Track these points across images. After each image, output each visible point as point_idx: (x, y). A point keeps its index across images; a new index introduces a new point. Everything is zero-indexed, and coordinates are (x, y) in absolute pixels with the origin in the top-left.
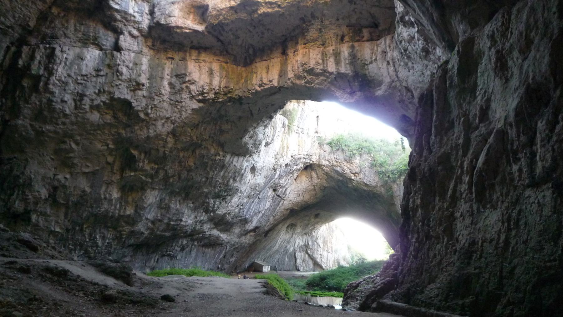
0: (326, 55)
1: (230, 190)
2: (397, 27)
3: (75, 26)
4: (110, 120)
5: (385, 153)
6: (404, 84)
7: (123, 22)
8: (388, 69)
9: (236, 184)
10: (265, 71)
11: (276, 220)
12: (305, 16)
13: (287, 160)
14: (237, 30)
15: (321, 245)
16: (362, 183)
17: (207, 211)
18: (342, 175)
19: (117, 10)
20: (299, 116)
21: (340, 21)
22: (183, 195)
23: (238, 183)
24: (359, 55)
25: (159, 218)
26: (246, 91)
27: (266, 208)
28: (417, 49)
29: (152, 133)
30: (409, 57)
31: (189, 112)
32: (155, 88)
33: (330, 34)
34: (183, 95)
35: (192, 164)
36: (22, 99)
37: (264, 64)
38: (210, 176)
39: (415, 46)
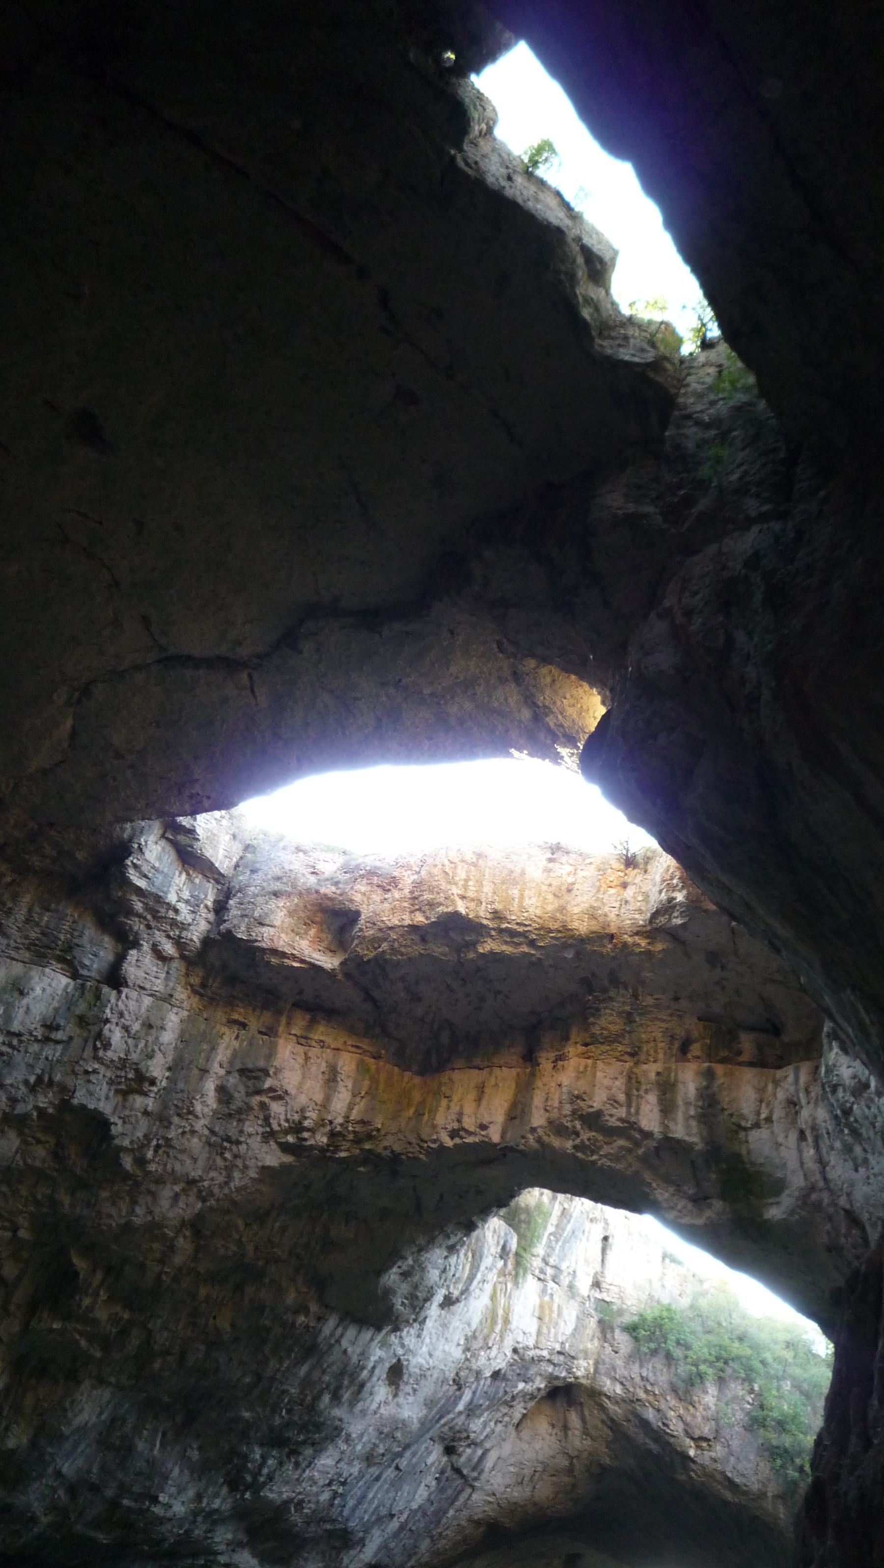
0: (639, 1082)
1: (318, 1427)
2: (826, 1047)
3: (30, 910)
4: (44, 1161)
5: (797, 1386)
6: (843, 1201)
7: (145, 918)
8: (800, 1151)
9: (337, 1412)
10: (472, 1095)
11: (437, 1553)
12: (593, 974)
13: (498, 1358)
14: (417, 982)
16: (718, 1477)
17: (235, 1484)
18: (660, 1437)
19: (139, 891)
20: (551, 1229)
21: (684, 1003)
22: (178, 1419)
23: (345, 1406)
24: (725, 1099)
25: (94, 1478)
26: (414, 1141)
27: (414, 1506)
28: (875, 1117)
29: (140, 1217)
30: (855, 1133)
31: (253, 1173)
32: (179, 1096)
33: (653, 1032)
34: (247, 1123)
35: (224, 1324)
37: (474, 1077)
38: (268, 1372)
39: (869, 1108)
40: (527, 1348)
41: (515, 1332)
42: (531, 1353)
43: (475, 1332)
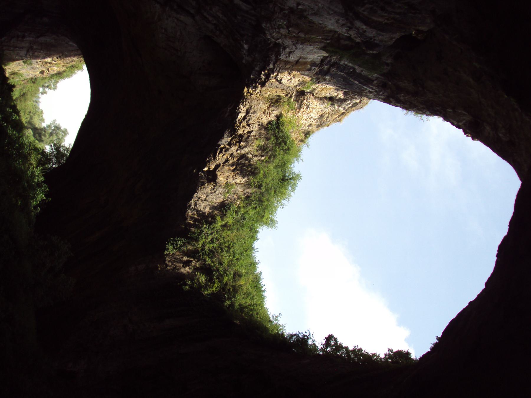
15: (42, 39)
20: (358, 70)
40: (278, 54)
41: (294, 47)
42: (273, 57)
43: (306, 18)
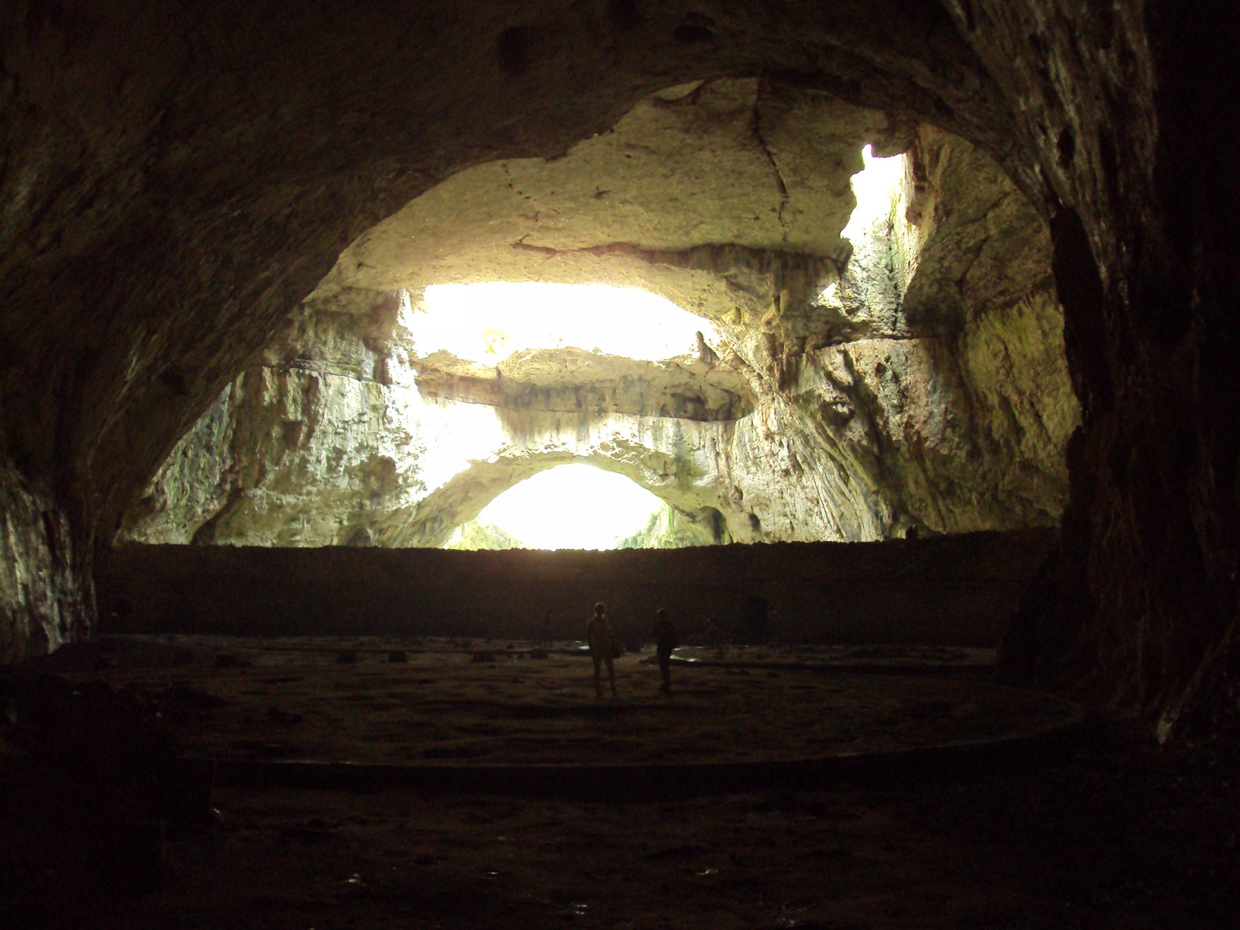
3: (335, 342)
6: (736, 483)
36: (268, 457)
